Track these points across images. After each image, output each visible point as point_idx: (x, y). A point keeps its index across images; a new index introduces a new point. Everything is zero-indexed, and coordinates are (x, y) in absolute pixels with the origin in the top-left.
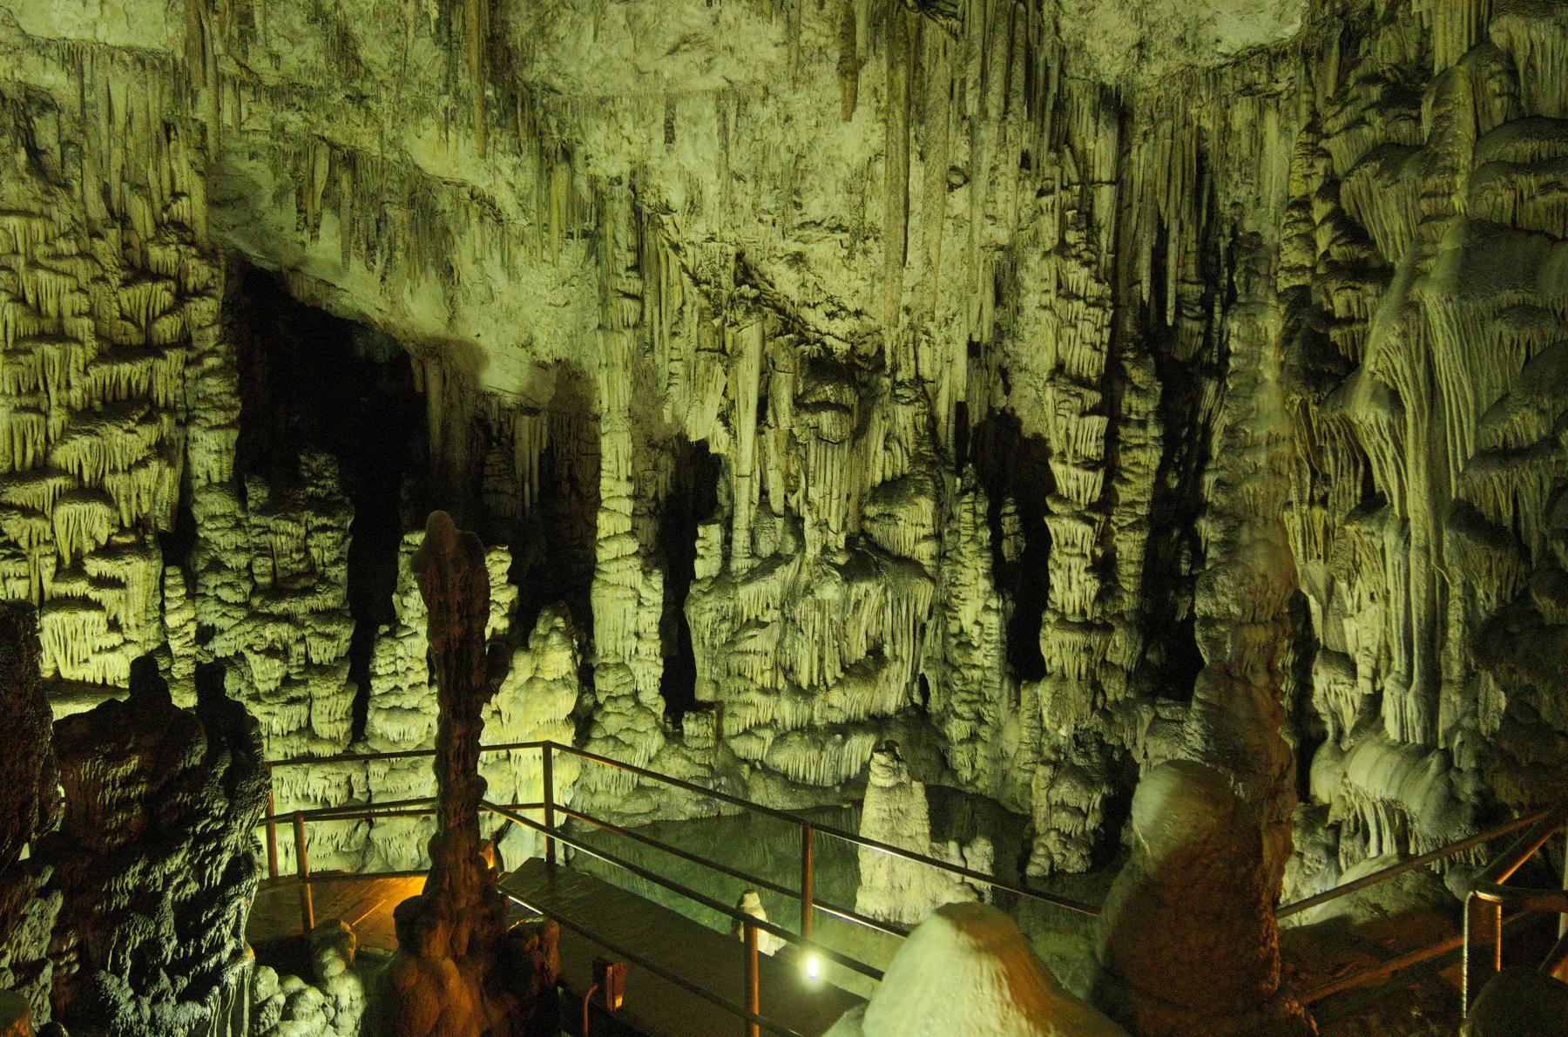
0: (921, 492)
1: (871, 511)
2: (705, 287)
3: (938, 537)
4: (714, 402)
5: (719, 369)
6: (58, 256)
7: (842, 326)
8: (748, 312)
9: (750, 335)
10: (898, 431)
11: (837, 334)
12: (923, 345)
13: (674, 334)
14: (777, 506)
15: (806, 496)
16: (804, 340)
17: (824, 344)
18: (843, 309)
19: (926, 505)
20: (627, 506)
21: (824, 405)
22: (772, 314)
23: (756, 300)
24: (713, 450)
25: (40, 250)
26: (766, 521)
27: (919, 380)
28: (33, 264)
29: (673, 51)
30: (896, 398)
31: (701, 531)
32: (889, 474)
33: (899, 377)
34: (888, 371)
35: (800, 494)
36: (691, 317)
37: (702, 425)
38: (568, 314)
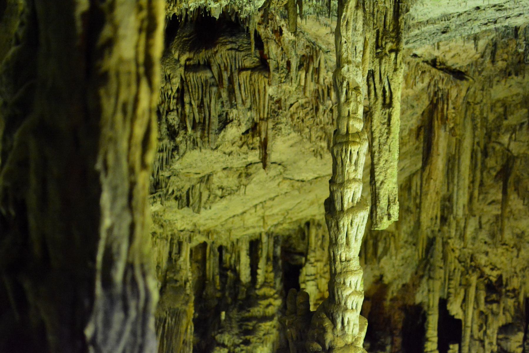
0: (519, 330)
1: (501, 336)
2: (463, 264)
3: (523, 346)
4: (459, 300)
5: (463, 291)
6: (324, 273)
7: (495, 273)
8: (473, 271)
9: (474, 279)
10: (508, 308)
11: (493, 275)
12: (515, 277)
13: (450, 279)
14: (476, 337)
15: (485, 332)
16: (486, 279)
17: (489, 279)
18: (496, 267)
19: (521, 335)
20: (436, 339)
21: (493, 302)
22: (479, 271)
23: (475, 267)
24: (457, 317)
25: (322, 272)
26: (474, 342)
27: (514, 290)
28: (321, 277)
29: (490, 204)
30: (508, 296)
31: (451, 346)
32: (504, 322)
33: (508, 288)
34: (504, 286)
35: (482, 332)
36: (458, 274)
37: (455, 309)
38: (402, 269)
